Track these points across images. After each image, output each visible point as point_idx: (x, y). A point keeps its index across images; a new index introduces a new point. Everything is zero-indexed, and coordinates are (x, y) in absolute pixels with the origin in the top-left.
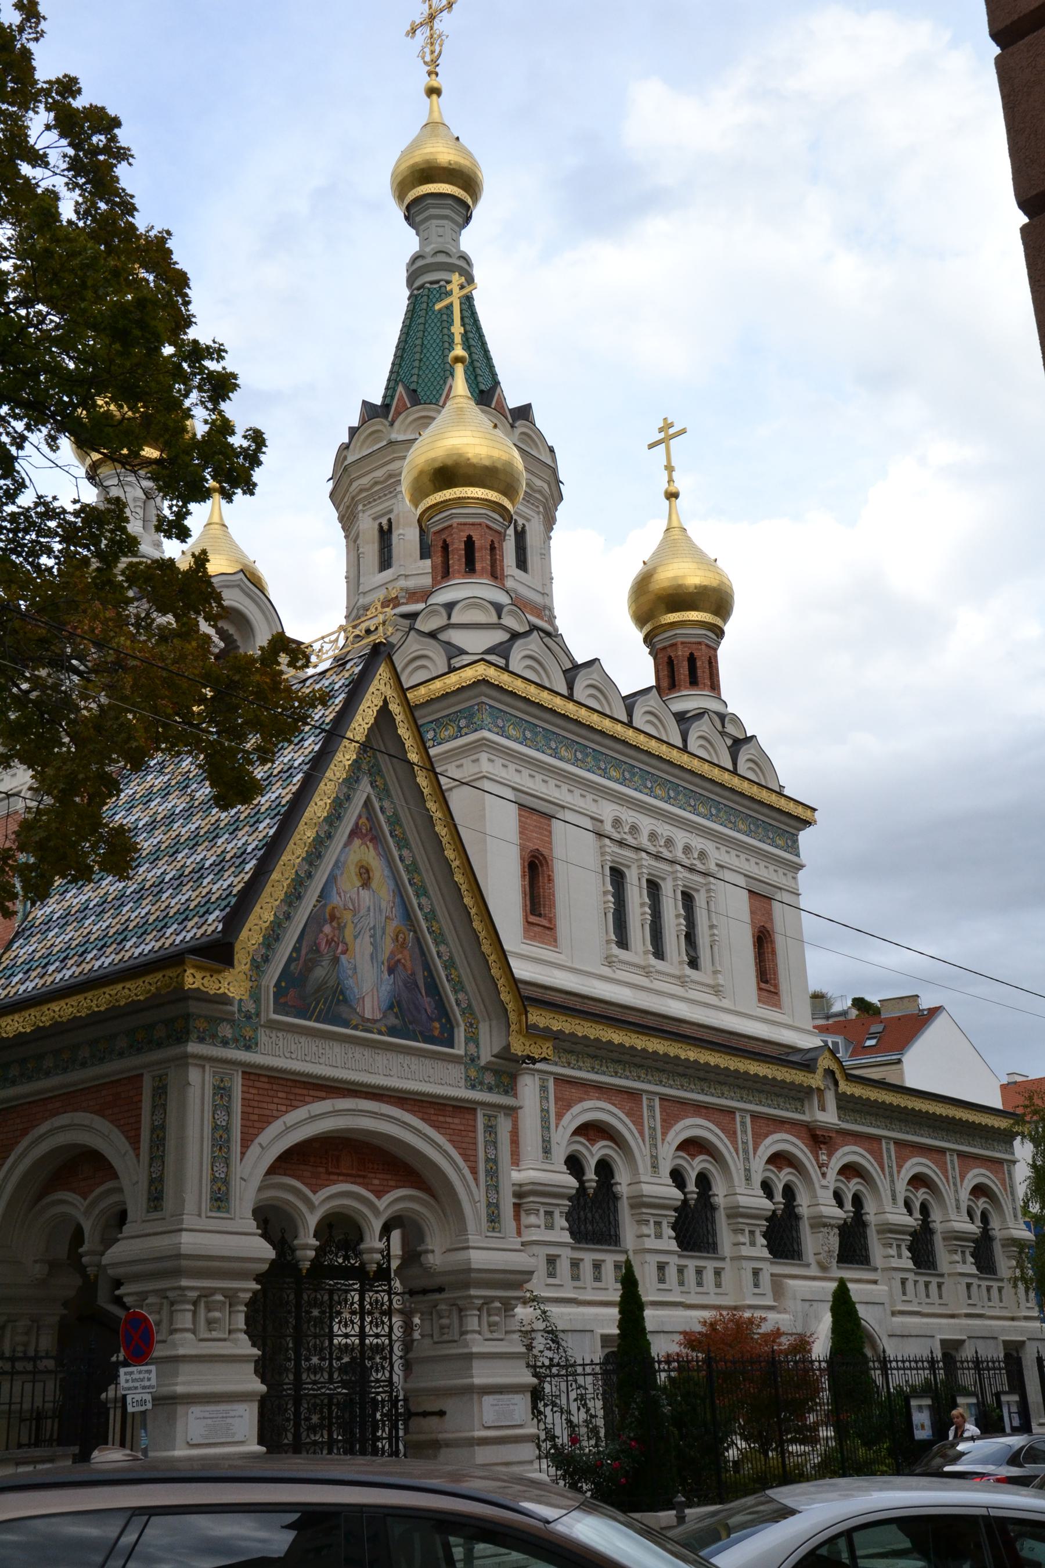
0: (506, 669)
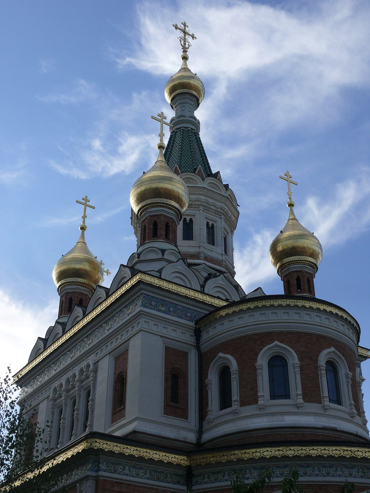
0: (160, 278)
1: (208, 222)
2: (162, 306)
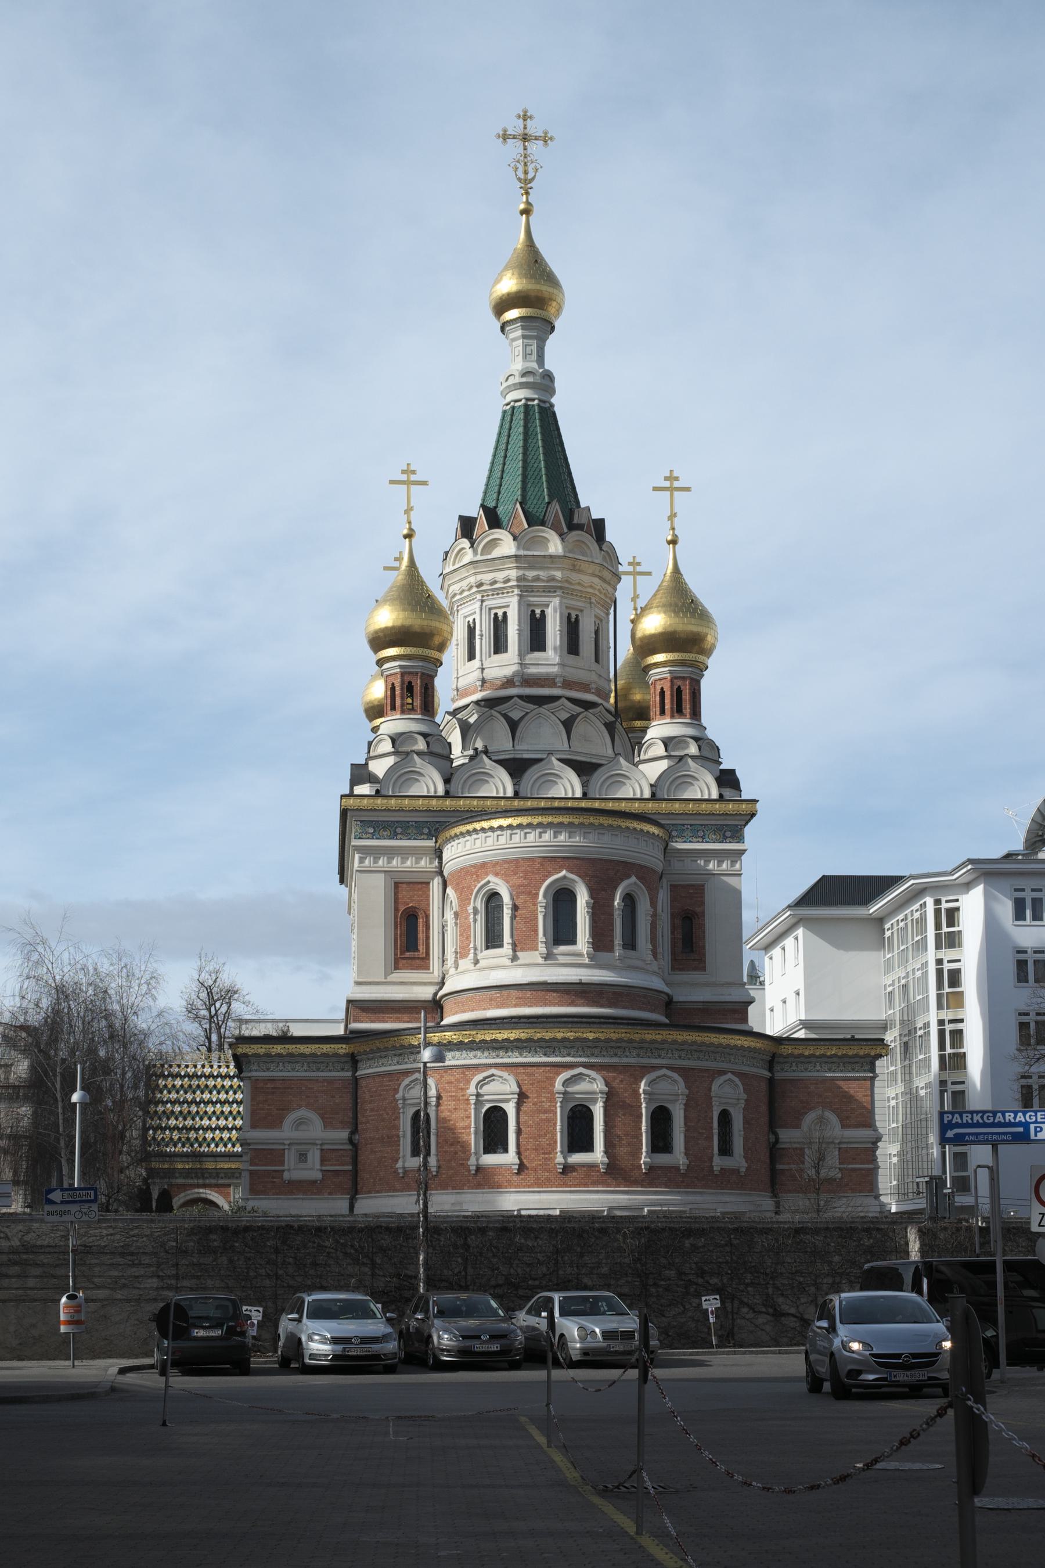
1: (533, 612)
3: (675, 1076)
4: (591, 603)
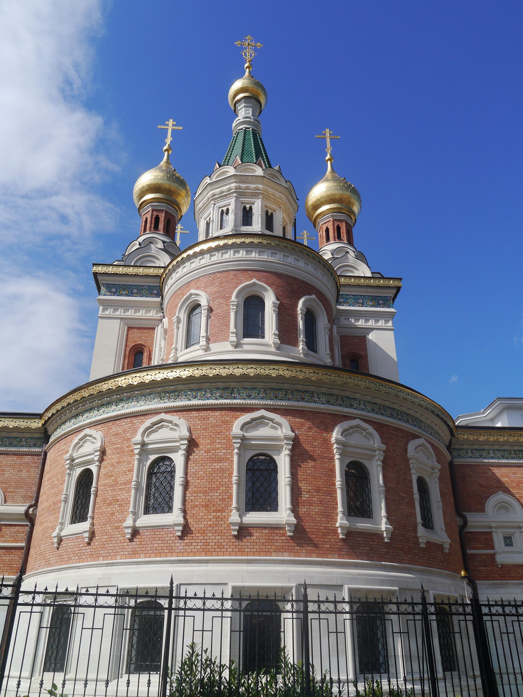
1: (245, 208)
2: (124, 291)
3: (370, 428)
4: (280, 208)
